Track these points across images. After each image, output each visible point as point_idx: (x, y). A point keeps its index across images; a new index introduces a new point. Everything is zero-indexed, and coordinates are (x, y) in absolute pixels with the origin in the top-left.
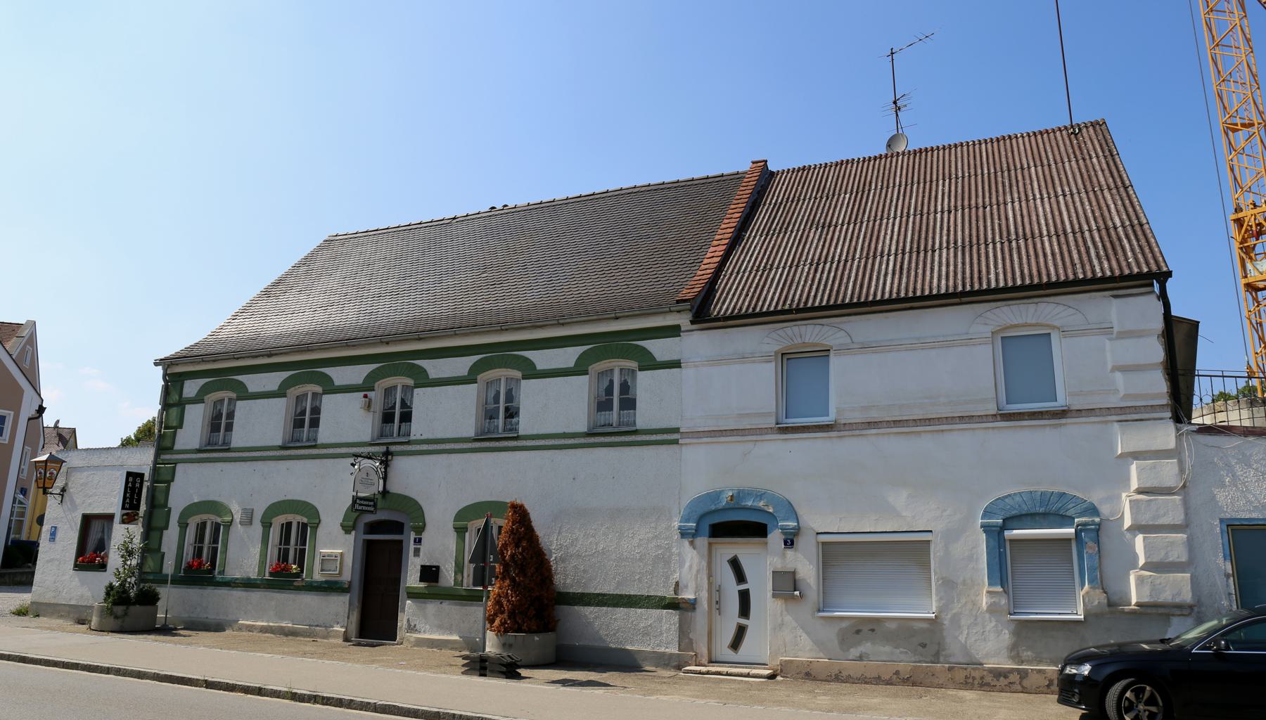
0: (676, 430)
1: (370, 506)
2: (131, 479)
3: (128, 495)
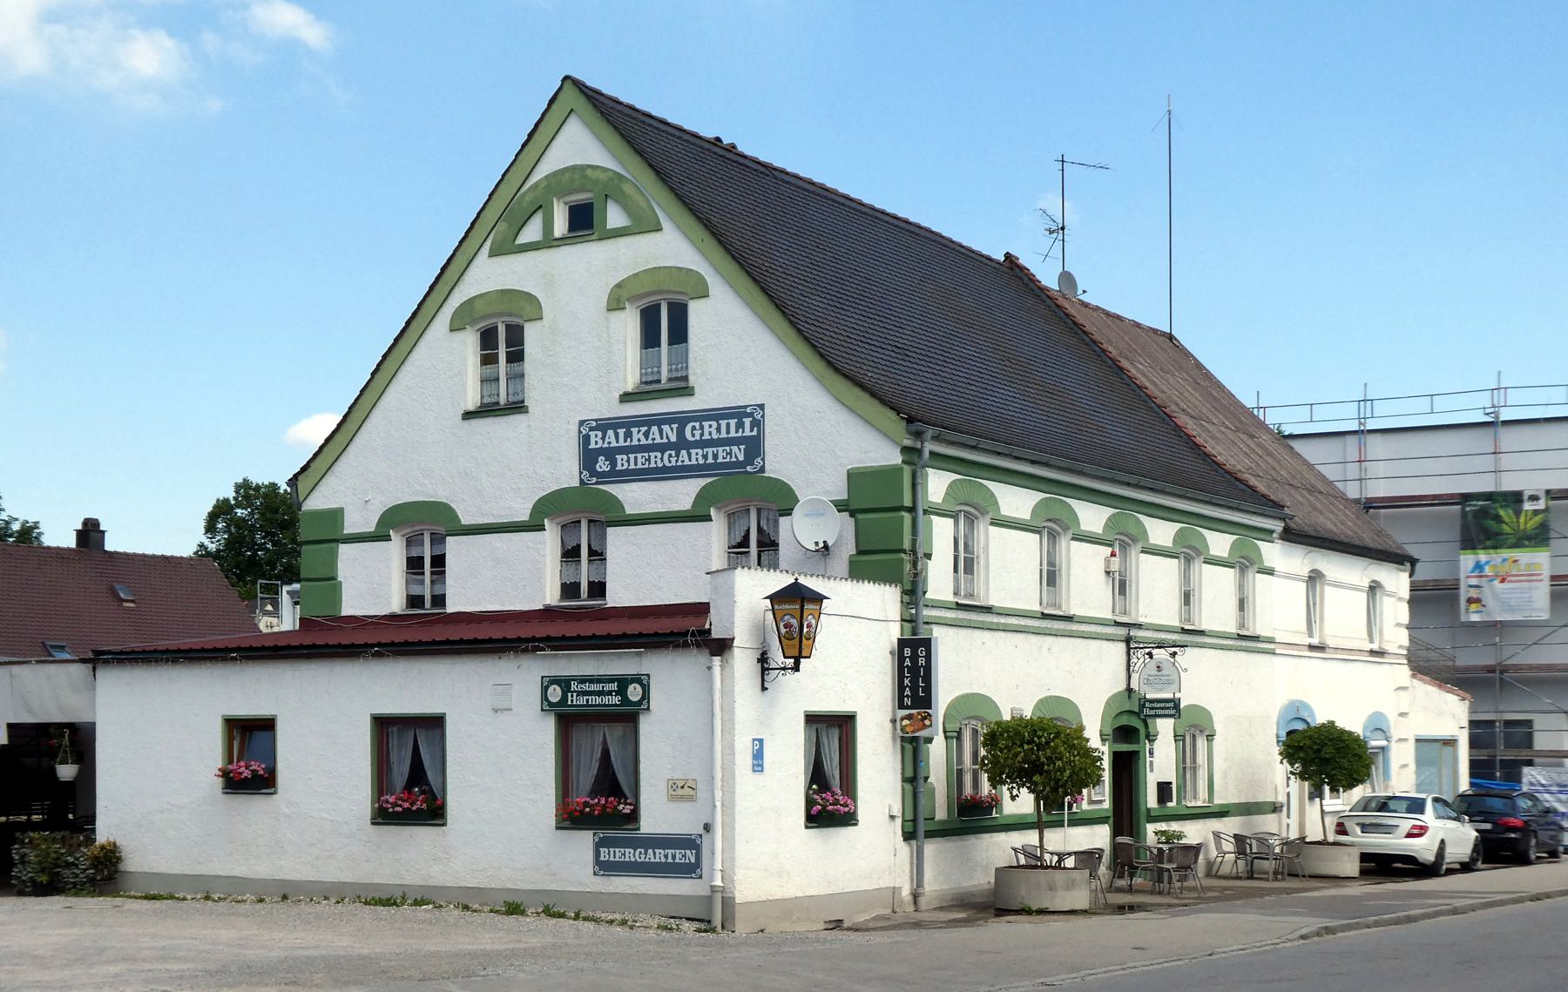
0: (1271, 641)
1: (1169, 708)
2: (907, 652)
3: (907, 682)
